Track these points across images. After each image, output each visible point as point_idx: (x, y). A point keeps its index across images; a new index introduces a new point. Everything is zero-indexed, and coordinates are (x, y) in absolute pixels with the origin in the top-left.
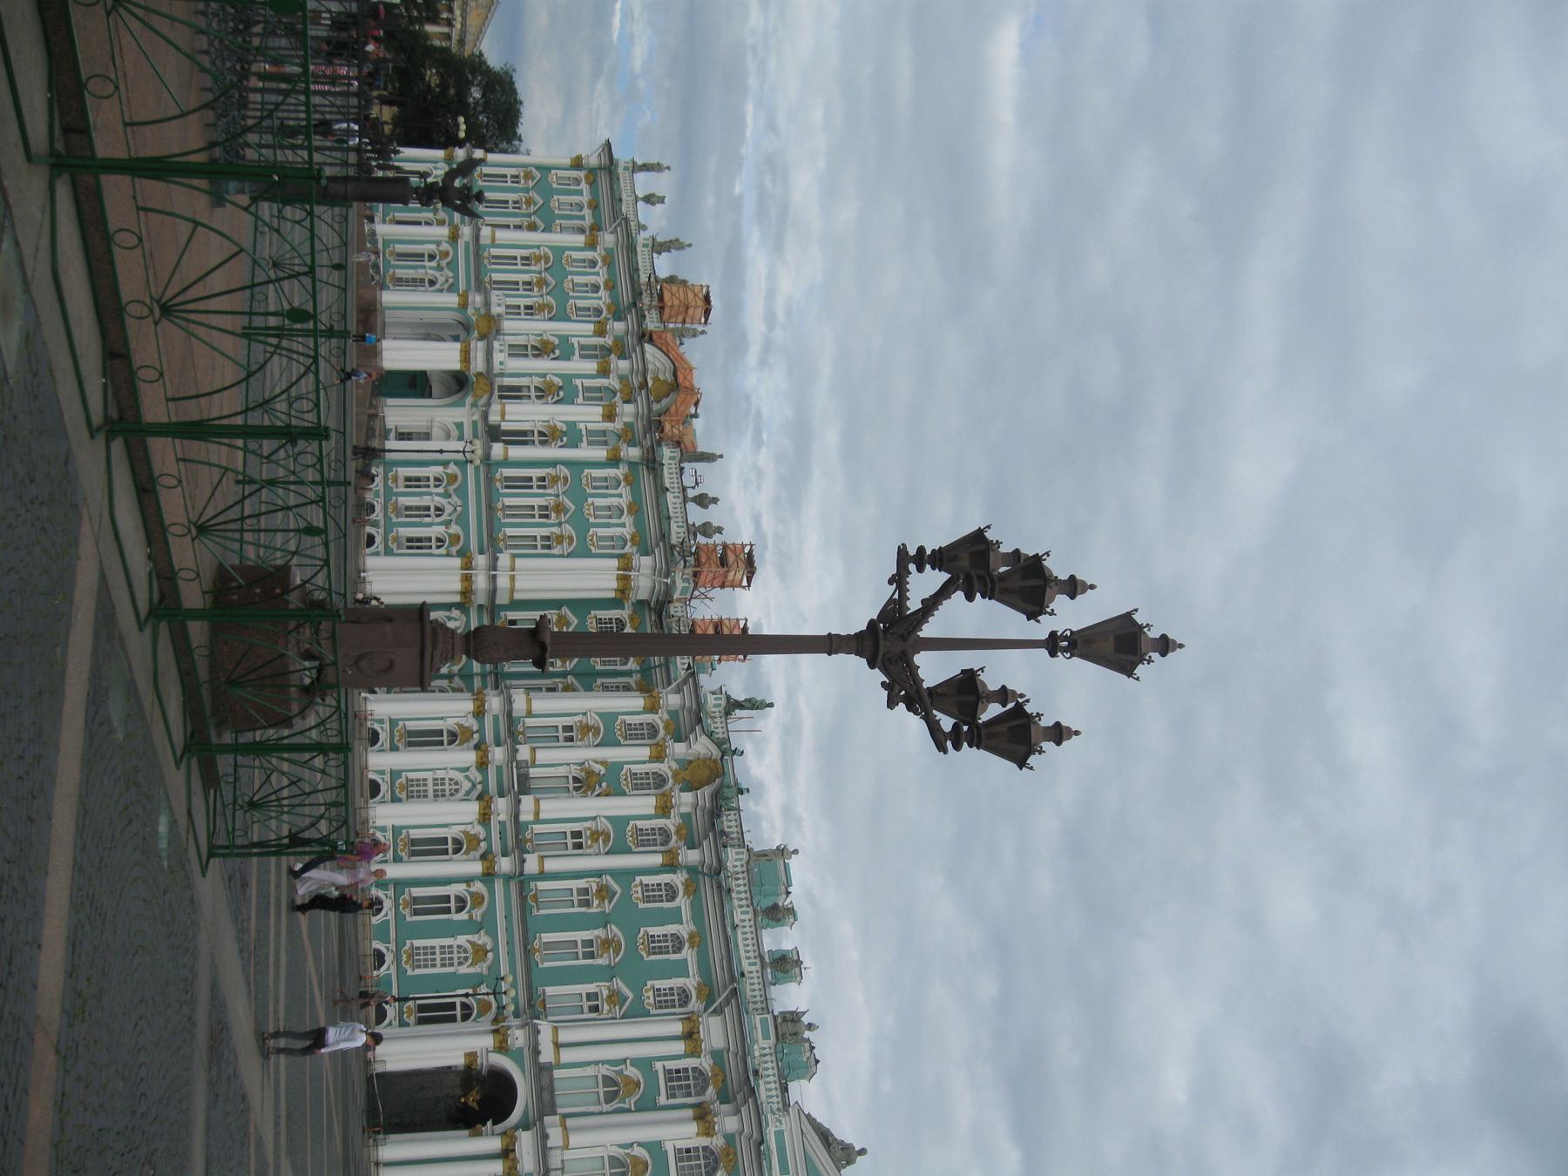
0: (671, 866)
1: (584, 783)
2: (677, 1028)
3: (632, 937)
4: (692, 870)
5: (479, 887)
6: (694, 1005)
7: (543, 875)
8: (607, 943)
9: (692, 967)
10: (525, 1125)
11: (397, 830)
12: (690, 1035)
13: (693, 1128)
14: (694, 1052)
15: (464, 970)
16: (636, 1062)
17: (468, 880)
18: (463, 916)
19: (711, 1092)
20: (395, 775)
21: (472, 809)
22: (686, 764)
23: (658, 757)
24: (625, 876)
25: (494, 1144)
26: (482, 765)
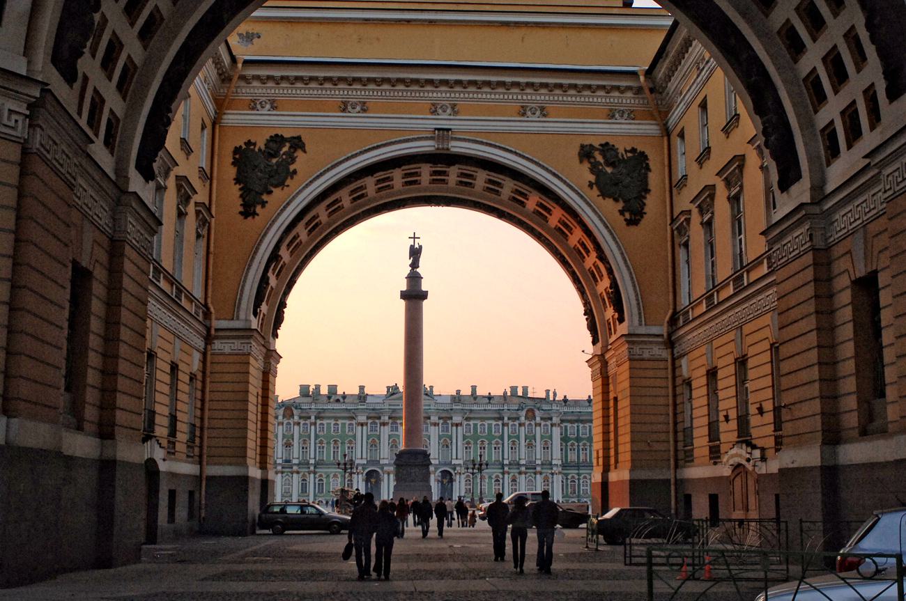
0: (315, 424)
1: (288, 445)
2: (360, 428)
3: (334, 437)
4: (316, 418)
5: (317, 476)
6: (354, 422)
7: (315, 458)
8: (336, 442)
9: (344, 421)
10: (382, 469)
11: (299, 496)
12: (362, 425)
13: (386, 427)
14: (367, 424)
15: (339, 480)
16: (368, 439)
17: (315, 478)
18: (325, 480)
19: (377, 421)
20: (282, 496)
21: (295, 475)
22: (284, 416)
23: (283, 424)
24: (316, 436)
25: (386, 476)
26: (282, 473)
